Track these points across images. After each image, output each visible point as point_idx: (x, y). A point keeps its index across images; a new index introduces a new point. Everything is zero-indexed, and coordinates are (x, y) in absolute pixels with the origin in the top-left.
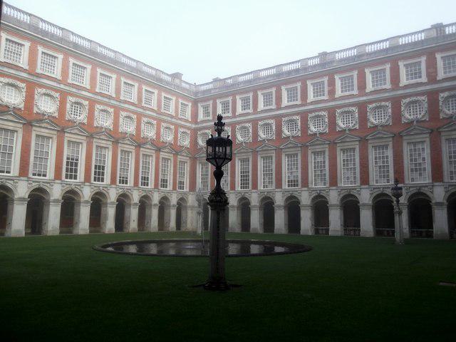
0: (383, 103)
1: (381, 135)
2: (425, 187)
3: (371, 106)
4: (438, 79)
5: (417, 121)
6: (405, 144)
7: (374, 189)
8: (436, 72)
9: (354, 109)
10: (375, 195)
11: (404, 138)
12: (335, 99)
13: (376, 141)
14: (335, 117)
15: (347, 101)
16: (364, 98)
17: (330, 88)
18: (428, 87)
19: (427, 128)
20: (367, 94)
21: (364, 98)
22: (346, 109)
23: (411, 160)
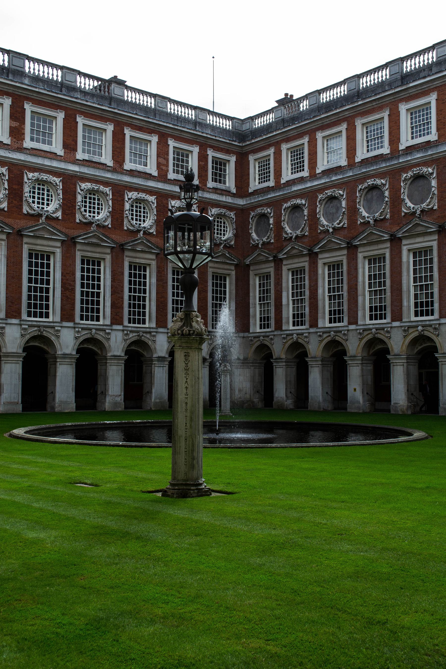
0: (102, 188)
1: (94, 240)
2: (146, 332)
3: (83, 186)
4: (169, 178)
5: (145, 233)
6: (126, 265)
7: (83, 329)
8: (167, 166)
9: (57, 180)
10: (81, 339)
11: (127, 253)
12: (21, 150)
13: (88, 248)
14: (21, 184)
15: (47, 162)
16: (76, 168)
17: (15, 124)
18: (160, 185)
19: (157, 247)
20: (76, 162)
21: (76, 168)
22: (45, 177)
23: (130, 289)
